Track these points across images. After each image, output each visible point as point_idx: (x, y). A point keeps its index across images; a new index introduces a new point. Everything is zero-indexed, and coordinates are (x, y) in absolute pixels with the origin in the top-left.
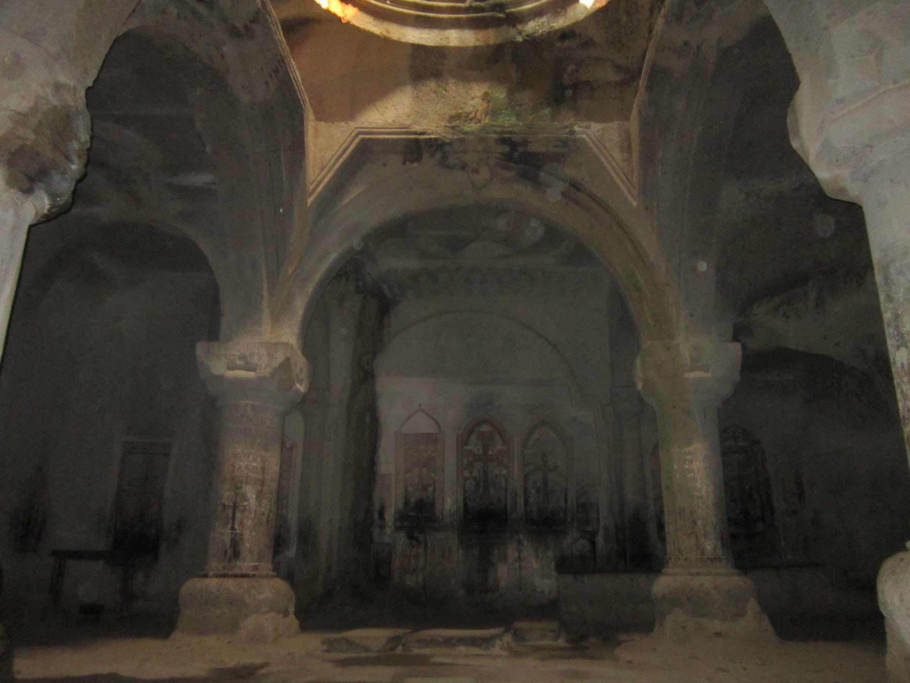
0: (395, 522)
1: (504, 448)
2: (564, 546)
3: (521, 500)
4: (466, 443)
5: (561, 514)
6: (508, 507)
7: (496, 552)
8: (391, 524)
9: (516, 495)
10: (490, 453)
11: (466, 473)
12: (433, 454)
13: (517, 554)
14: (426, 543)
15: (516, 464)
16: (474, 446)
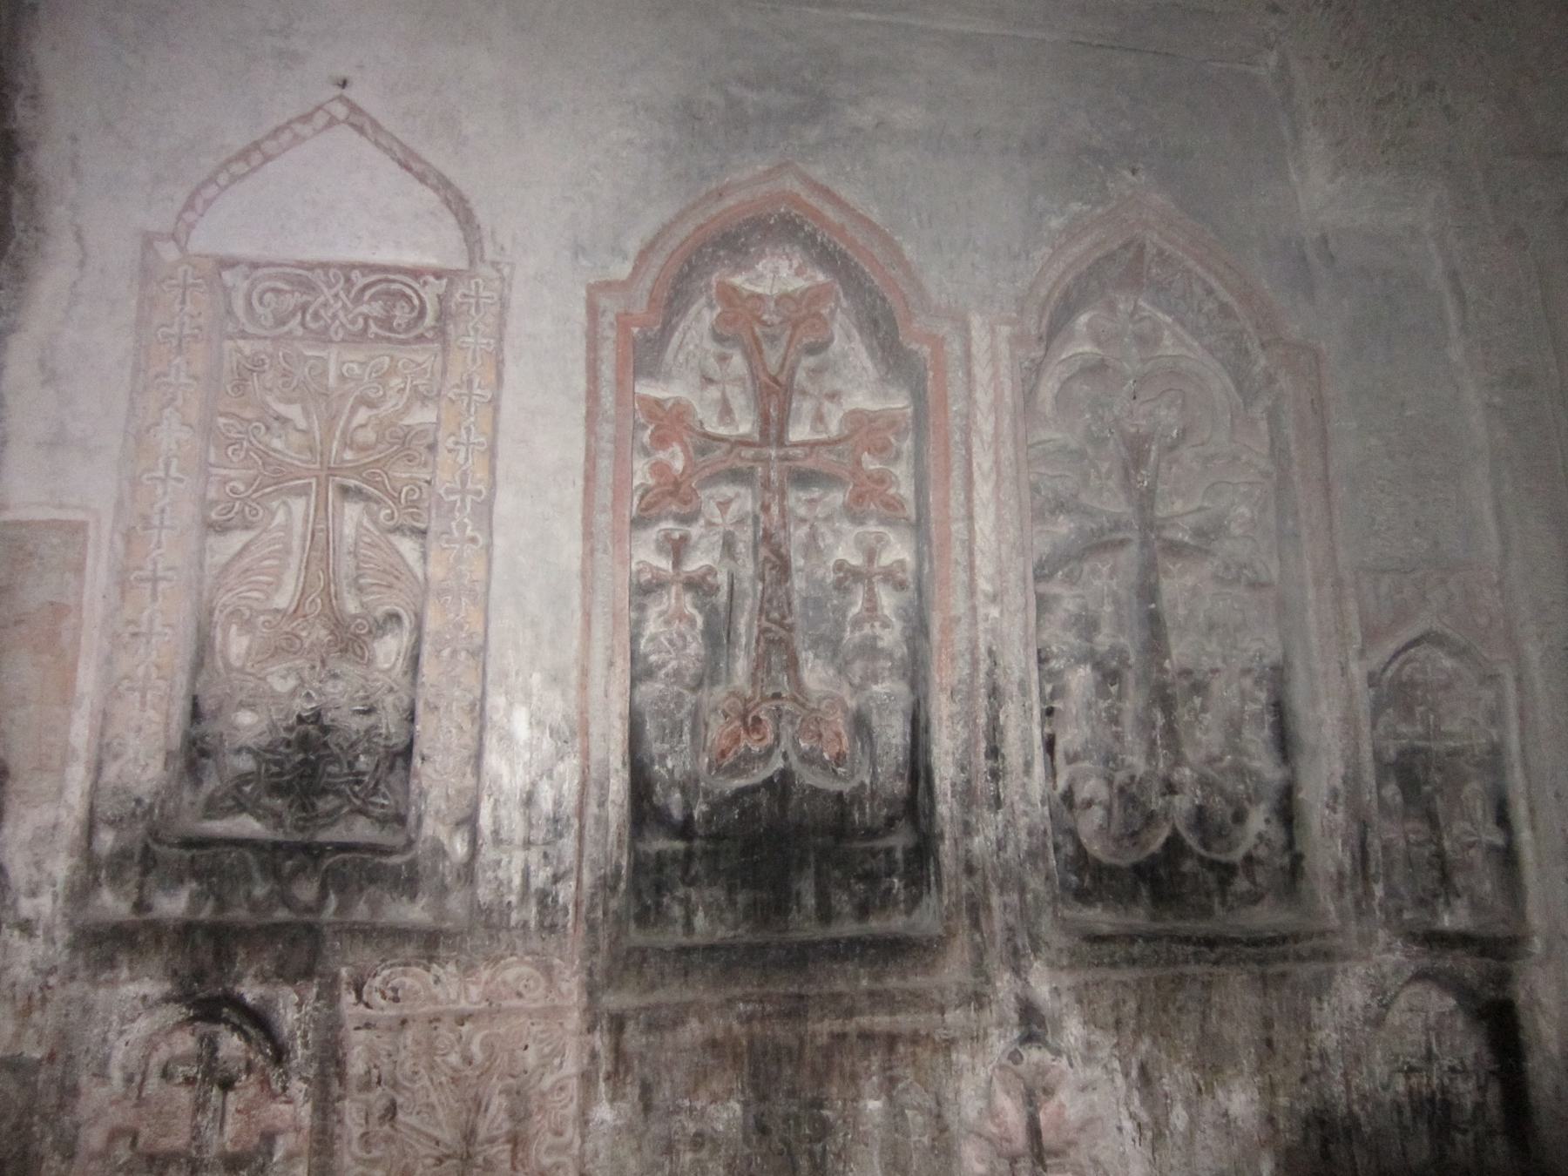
0: (80, 893)
1: (899, 402)
2: (1327, 1037)
3: (1022, 731)
4: (646, 353)
5: (1258, 821)
6: (945, 773)
7: (874, 1105)
8: (44, 906)
9: (994, 692)
10: (799, 432)
11: (648, 555)
12: (423, 416)
13: (1011, 1112)
14: (331, 1058)
15: (983, 491)
16: (703, 386)
